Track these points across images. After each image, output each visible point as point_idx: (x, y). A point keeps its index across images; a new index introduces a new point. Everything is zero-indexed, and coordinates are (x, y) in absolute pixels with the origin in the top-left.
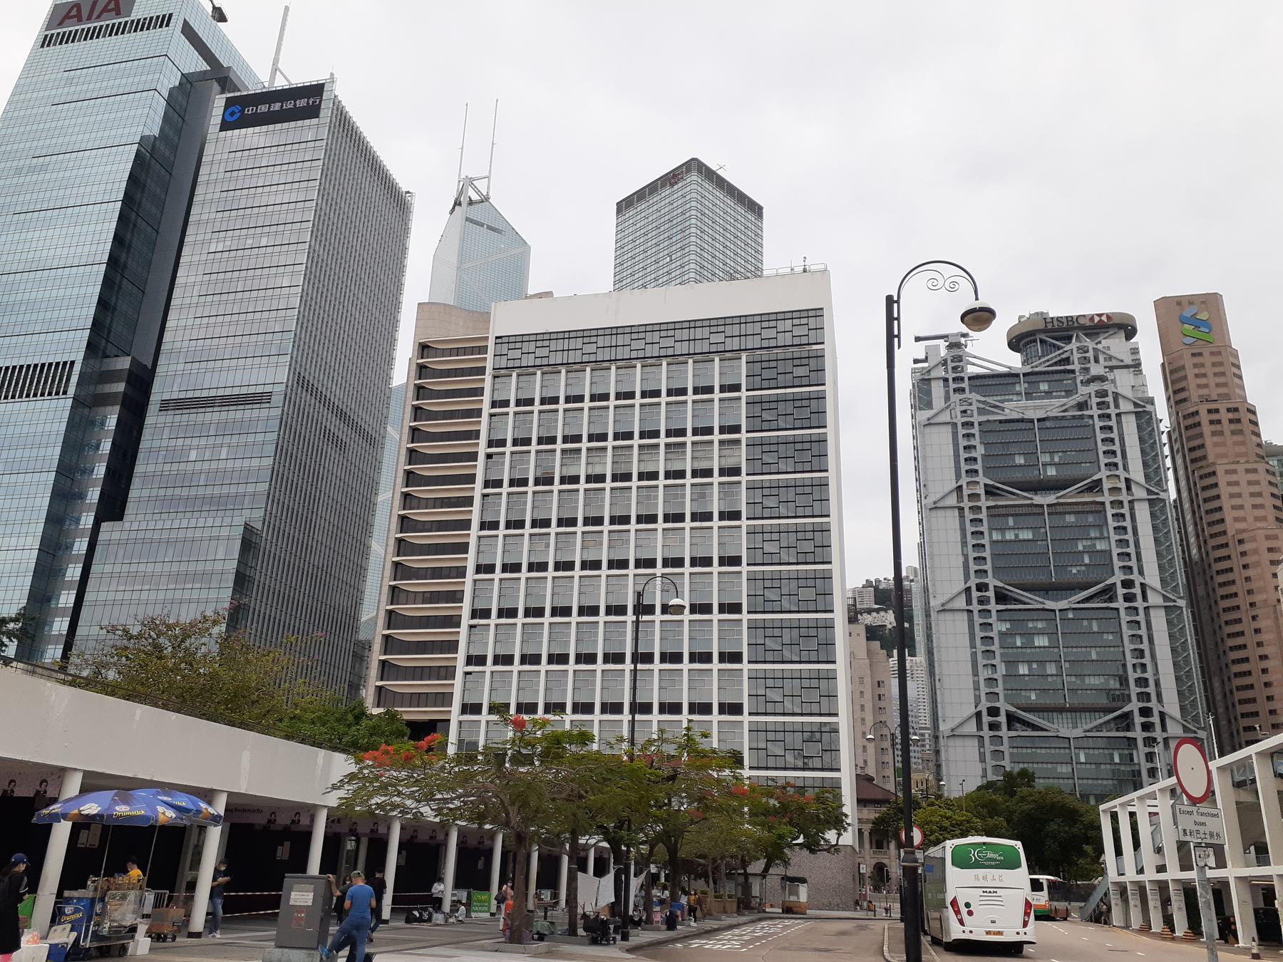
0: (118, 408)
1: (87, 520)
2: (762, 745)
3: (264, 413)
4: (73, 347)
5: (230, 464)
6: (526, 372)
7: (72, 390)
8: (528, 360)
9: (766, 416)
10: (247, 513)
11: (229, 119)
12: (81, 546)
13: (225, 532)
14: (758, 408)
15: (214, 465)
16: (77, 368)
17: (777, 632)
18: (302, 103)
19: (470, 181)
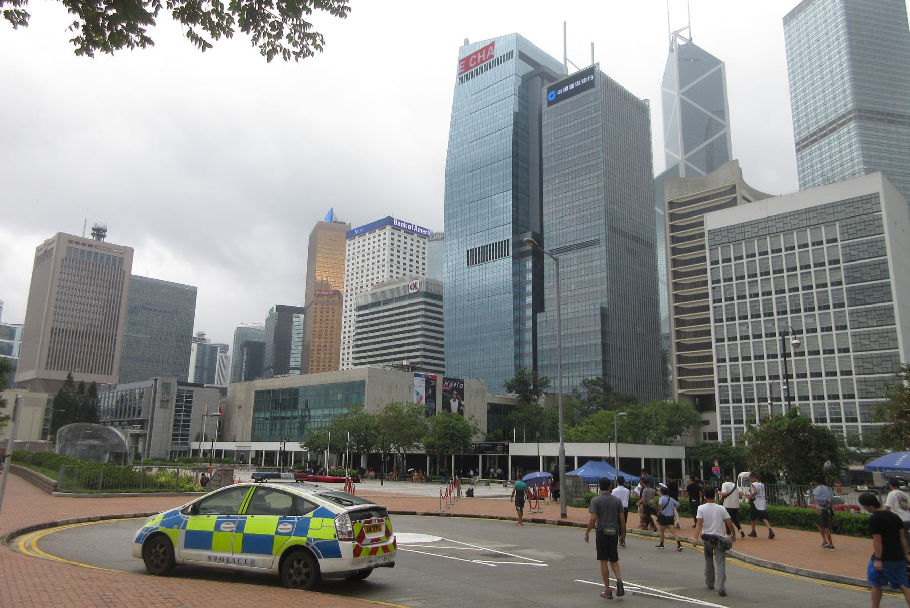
0: (531, 257)
1: (529, 312)
2: (867, 411)
3: (598, 250)
4: (506, 233)
5: (587, 278)
6: (725, 245)
7: (511, 254)
8: (725, 240)
9: (853, 253)
10: (599, 301)
11: (550, 99)
12: (529, 324)
13: (592, 312)
14: (848, 249)
15: (580, 279)
16: (511, 242)
17: (870, 360)
18: (584, 81)
19: (676, 34)
